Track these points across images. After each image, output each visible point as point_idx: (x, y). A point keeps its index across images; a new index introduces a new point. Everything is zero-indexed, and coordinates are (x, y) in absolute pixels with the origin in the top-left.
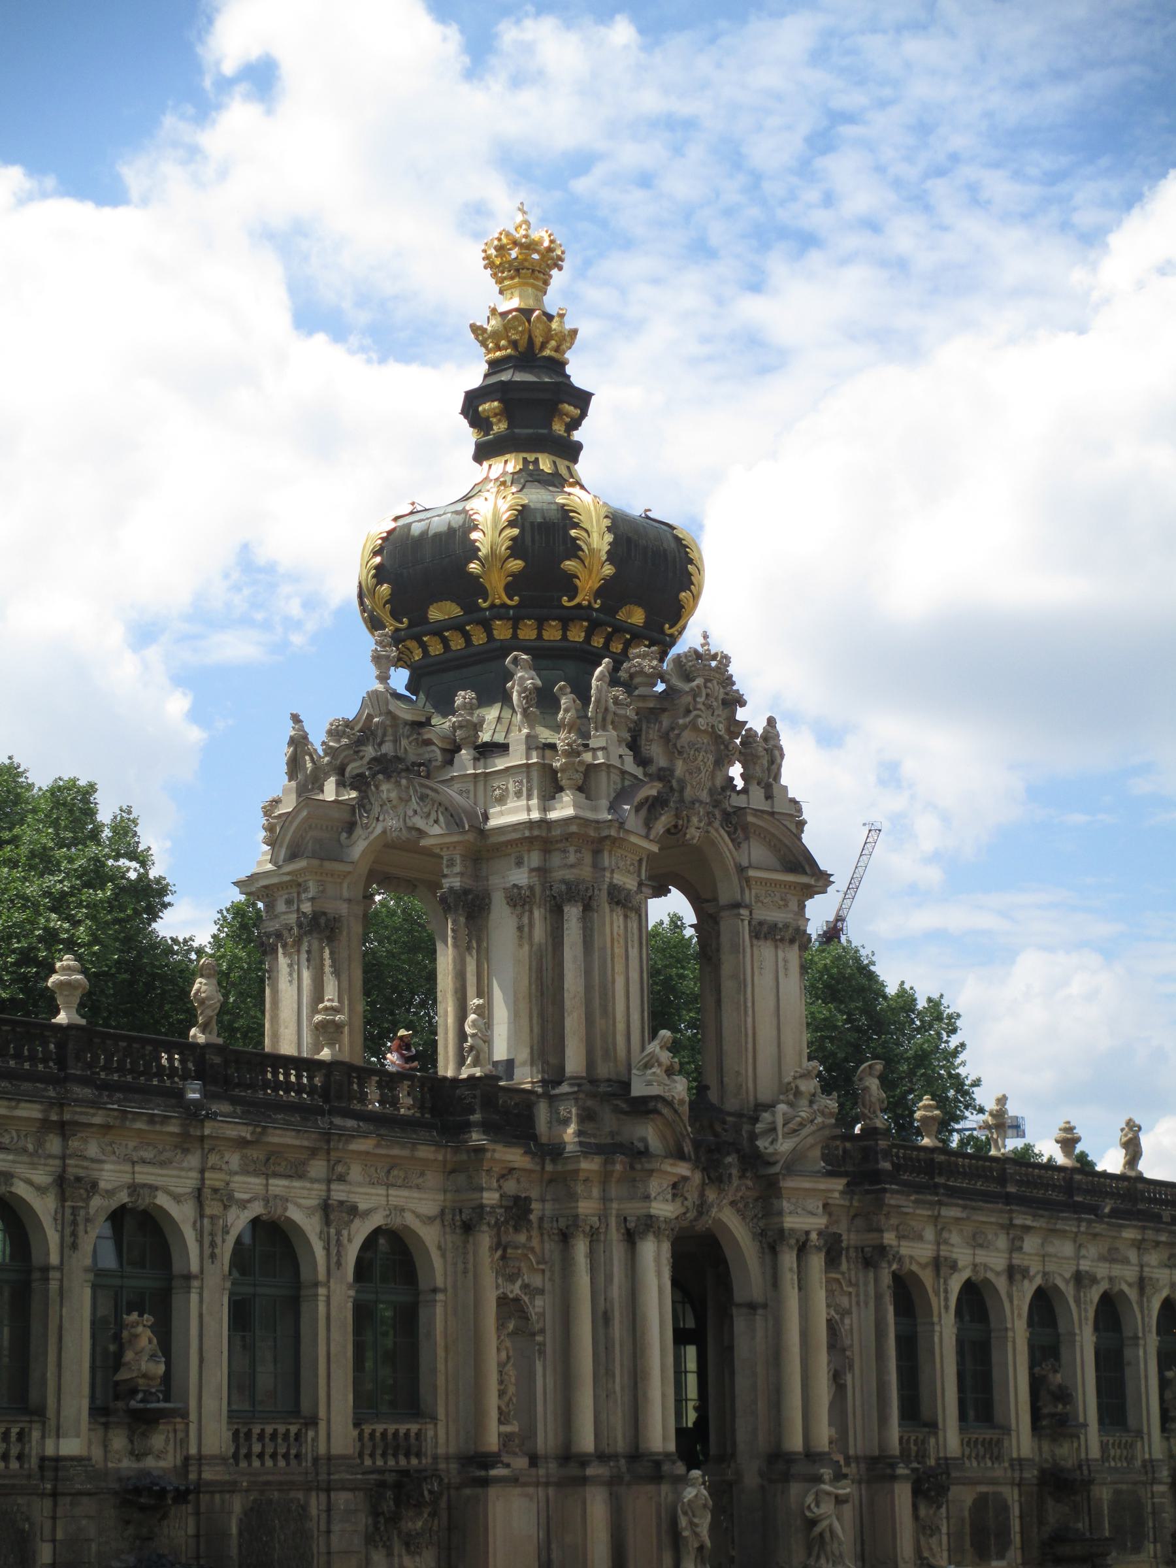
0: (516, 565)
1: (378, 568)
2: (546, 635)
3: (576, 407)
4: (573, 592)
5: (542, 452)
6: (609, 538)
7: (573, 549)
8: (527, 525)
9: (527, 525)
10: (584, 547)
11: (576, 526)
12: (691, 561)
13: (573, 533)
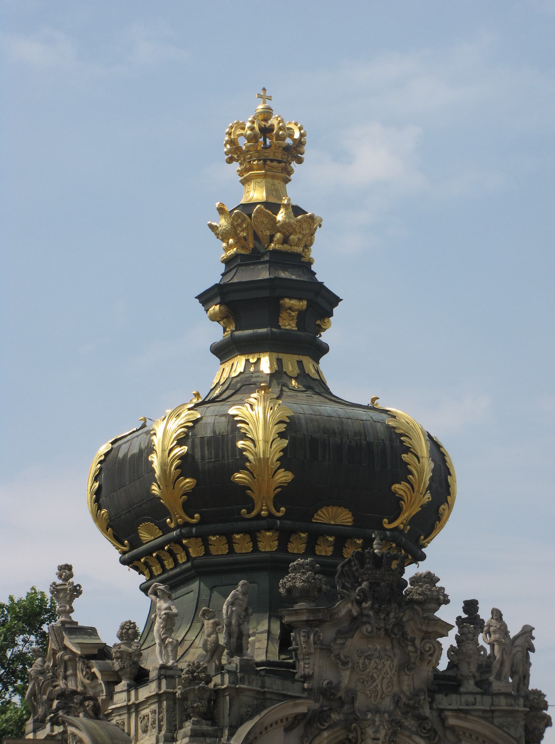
0: (188, 482)
1: (98, 493)
2: (237, 548)
3: (300, 299)
4: (250, 504)
5: (264, 352)
6: (285, 443)
7: (240, 461)
8: (197, 441)
9: (197, 441)
10: (251, 457)
11: (244, 437)
12: (407, 450)
13: (240, 444)
